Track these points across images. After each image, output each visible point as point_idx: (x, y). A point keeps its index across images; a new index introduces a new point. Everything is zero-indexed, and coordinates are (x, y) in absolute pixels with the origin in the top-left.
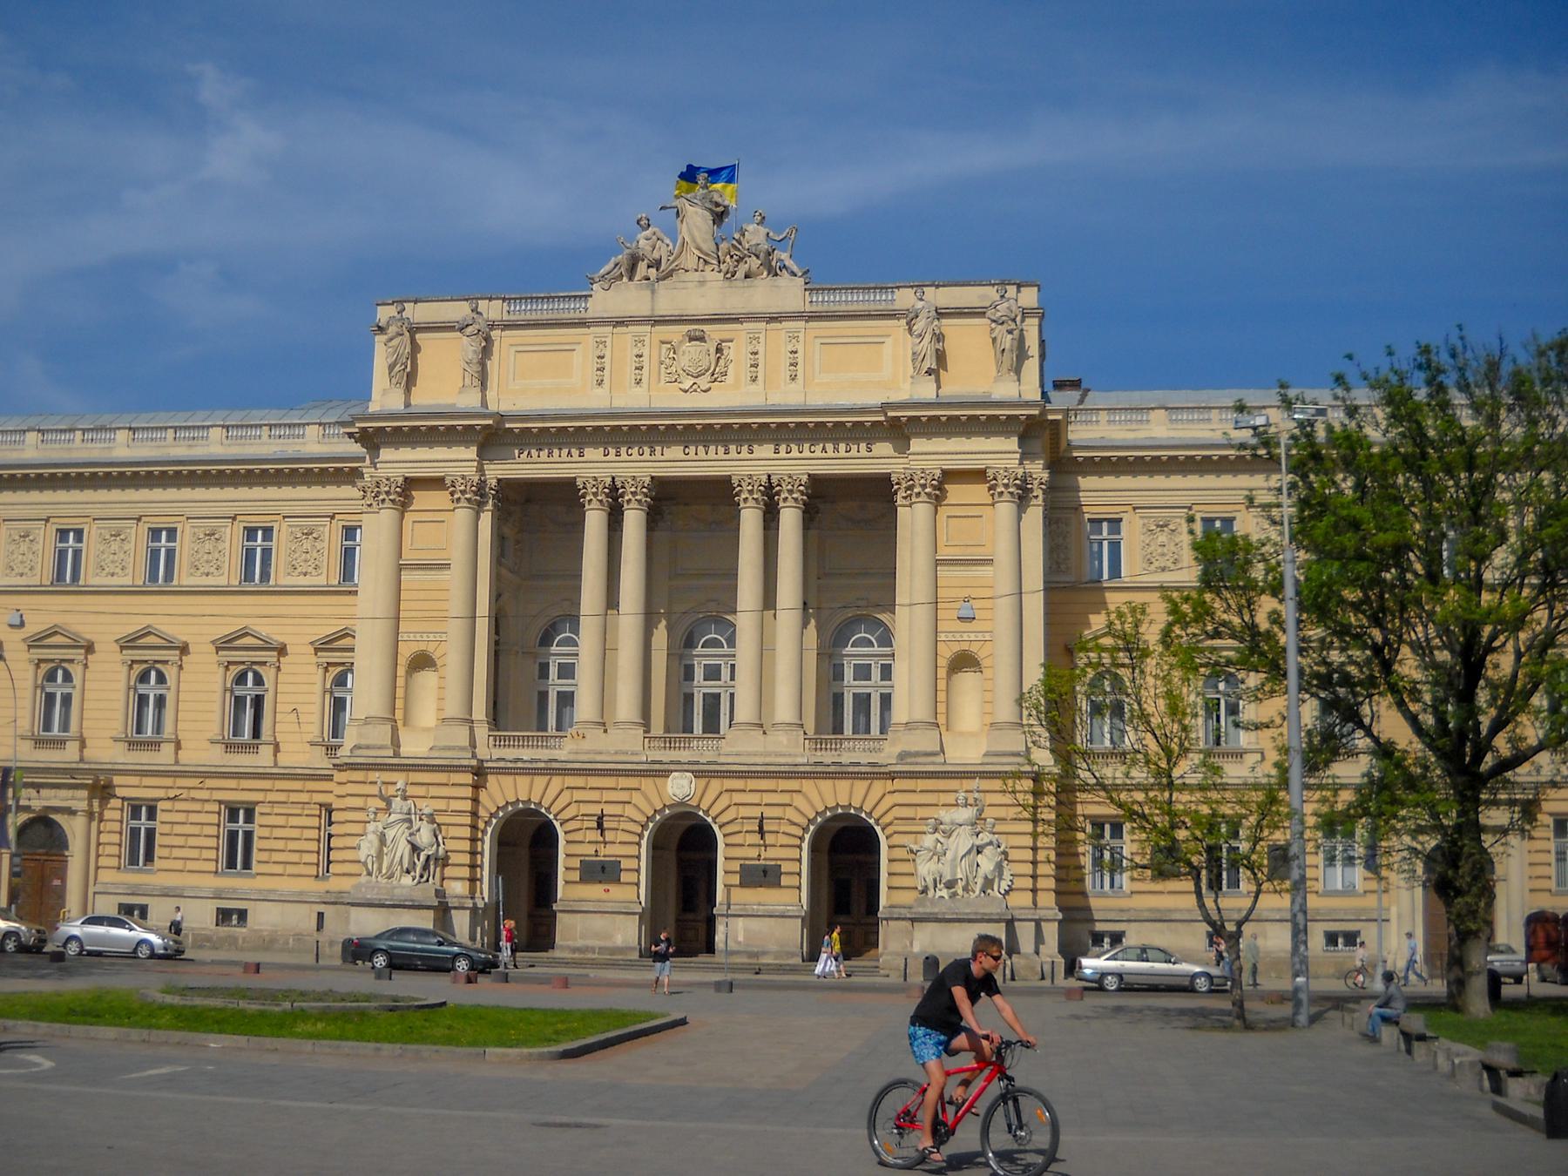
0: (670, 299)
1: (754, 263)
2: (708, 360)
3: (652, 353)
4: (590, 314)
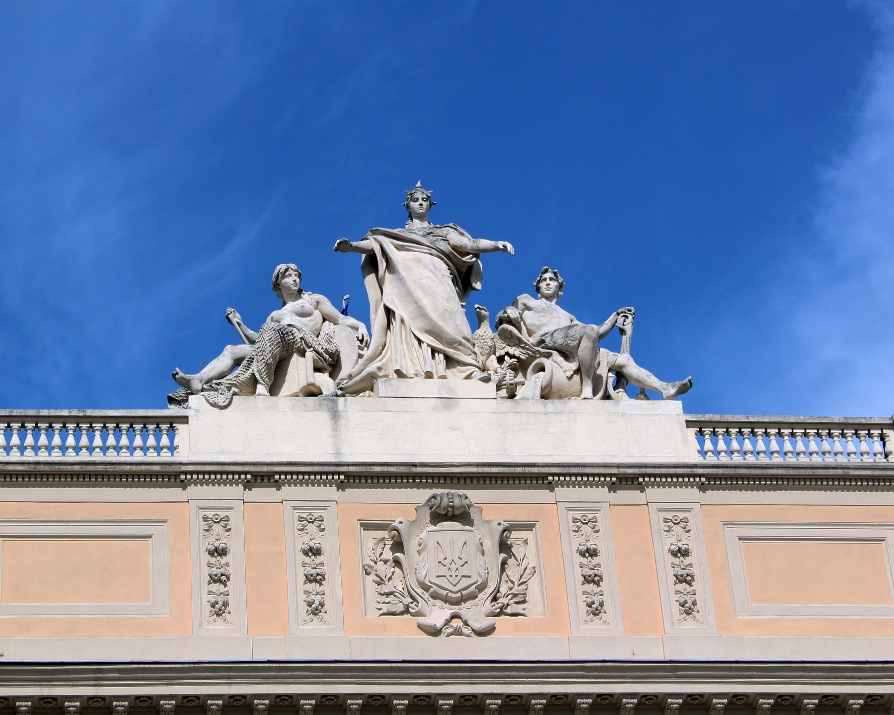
0: (370, 433)
1: (559, 369)
2: (483, 566)
3: (348, 548)
4: (183, 455)
